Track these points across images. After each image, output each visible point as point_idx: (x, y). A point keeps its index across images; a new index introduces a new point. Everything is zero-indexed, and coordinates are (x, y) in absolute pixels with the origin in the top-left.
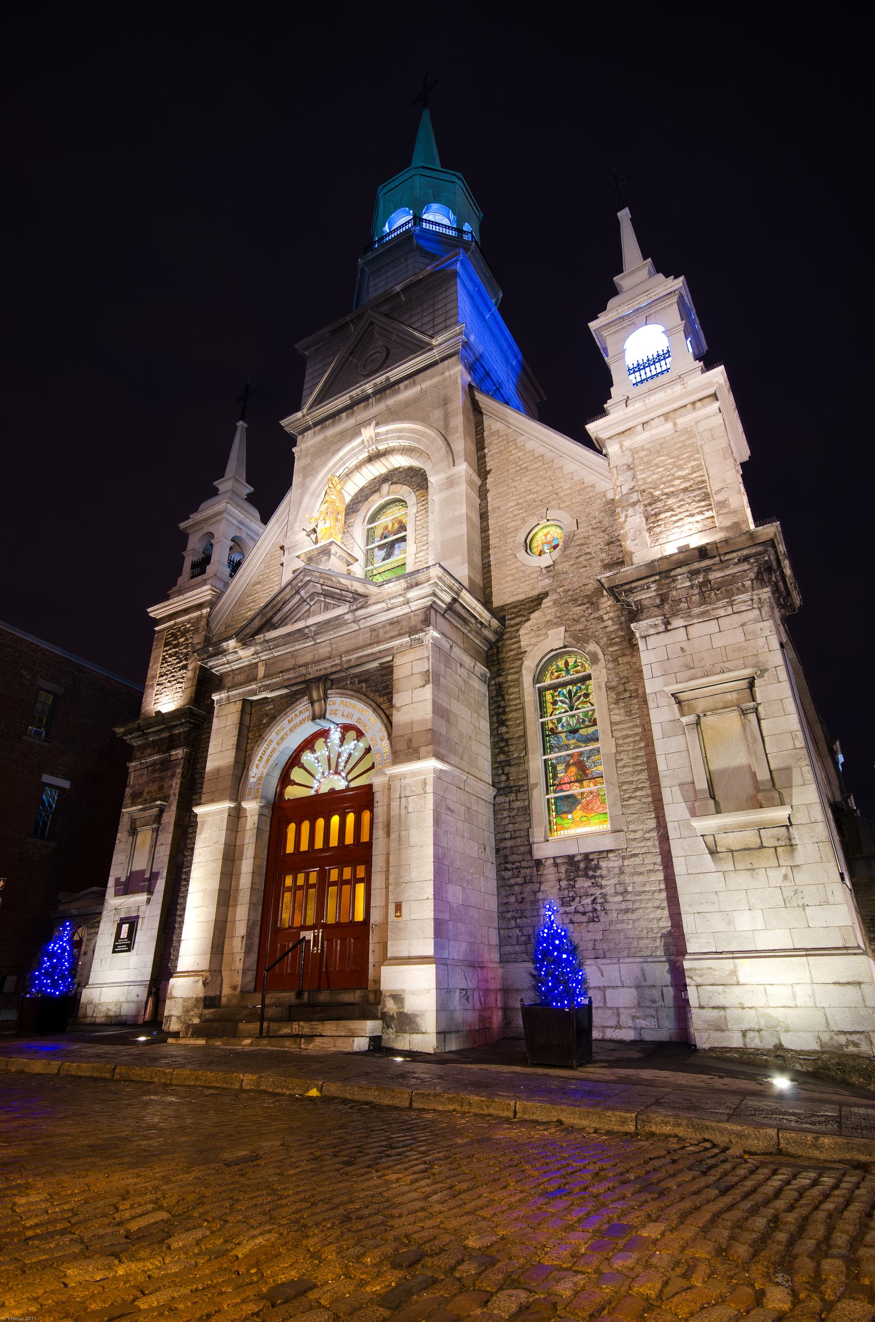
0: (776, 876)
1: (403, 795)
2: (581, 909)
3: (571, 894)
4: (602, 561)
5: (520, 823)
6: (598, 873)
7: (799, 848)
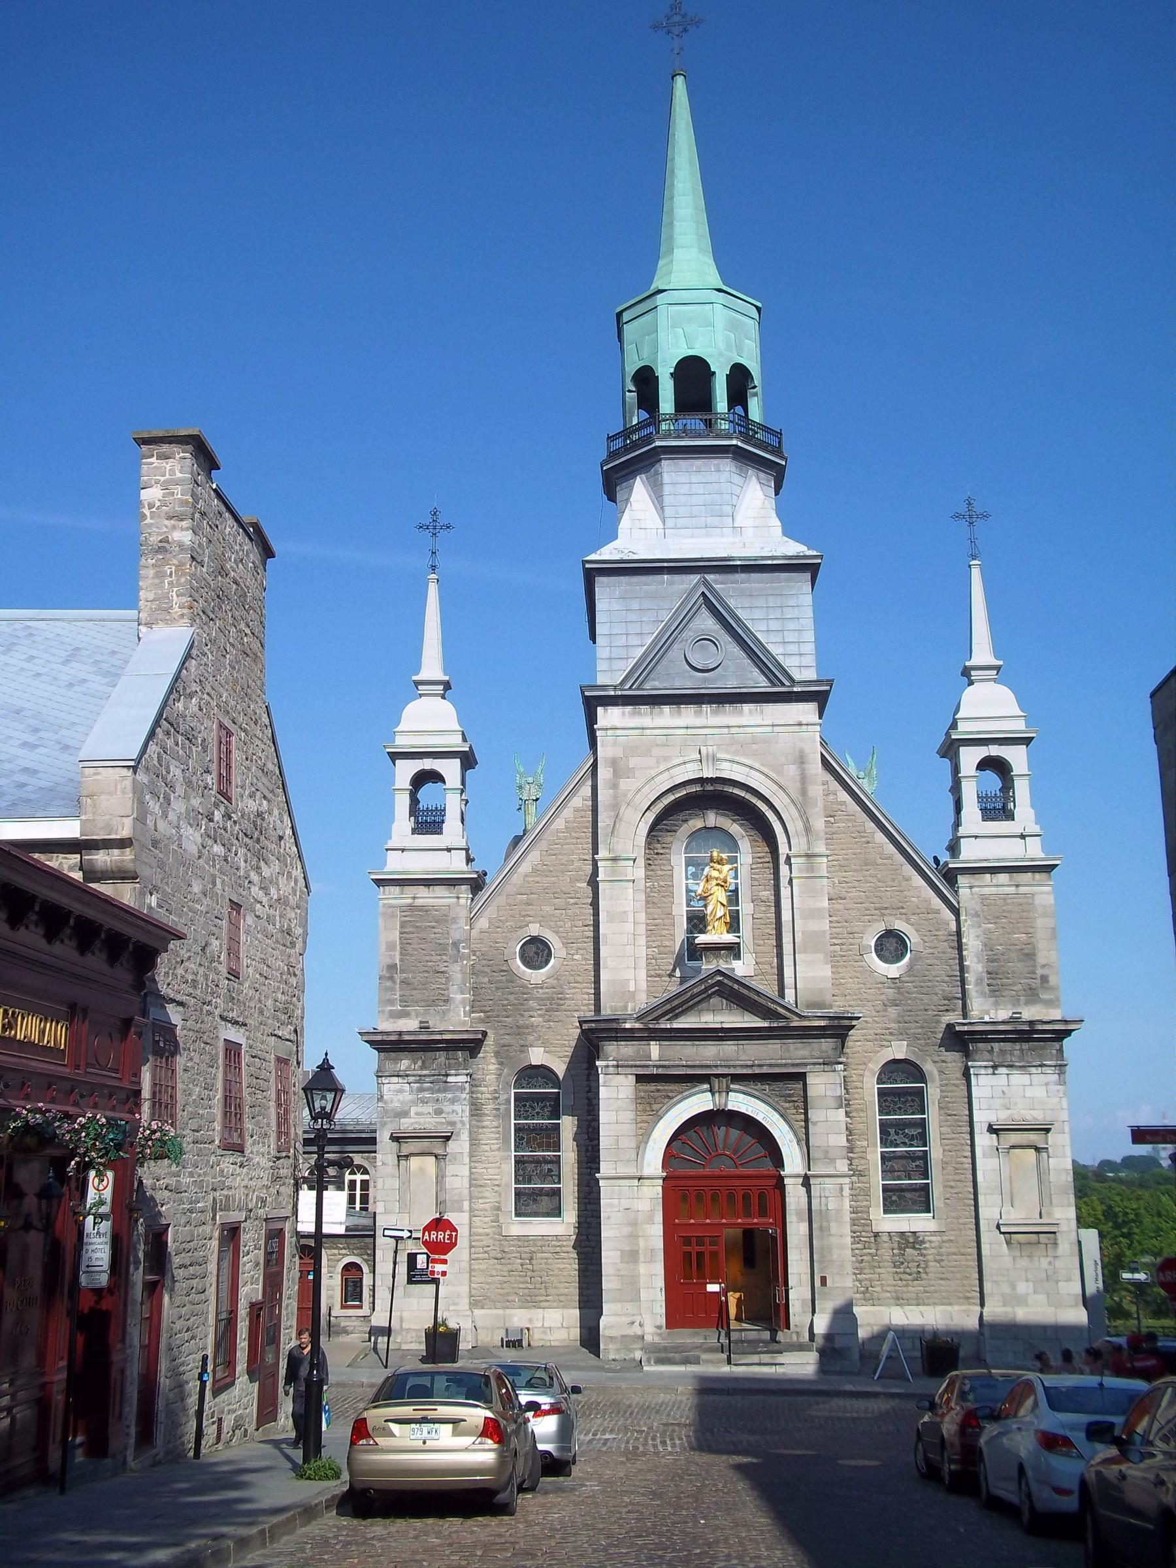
0: (1044, 1262)
1: (822, 1195)
2: (908, 1270)
3: (901, 1260)
4: (943, 990)
5: (862, 1201)
7: (1061, 1246)
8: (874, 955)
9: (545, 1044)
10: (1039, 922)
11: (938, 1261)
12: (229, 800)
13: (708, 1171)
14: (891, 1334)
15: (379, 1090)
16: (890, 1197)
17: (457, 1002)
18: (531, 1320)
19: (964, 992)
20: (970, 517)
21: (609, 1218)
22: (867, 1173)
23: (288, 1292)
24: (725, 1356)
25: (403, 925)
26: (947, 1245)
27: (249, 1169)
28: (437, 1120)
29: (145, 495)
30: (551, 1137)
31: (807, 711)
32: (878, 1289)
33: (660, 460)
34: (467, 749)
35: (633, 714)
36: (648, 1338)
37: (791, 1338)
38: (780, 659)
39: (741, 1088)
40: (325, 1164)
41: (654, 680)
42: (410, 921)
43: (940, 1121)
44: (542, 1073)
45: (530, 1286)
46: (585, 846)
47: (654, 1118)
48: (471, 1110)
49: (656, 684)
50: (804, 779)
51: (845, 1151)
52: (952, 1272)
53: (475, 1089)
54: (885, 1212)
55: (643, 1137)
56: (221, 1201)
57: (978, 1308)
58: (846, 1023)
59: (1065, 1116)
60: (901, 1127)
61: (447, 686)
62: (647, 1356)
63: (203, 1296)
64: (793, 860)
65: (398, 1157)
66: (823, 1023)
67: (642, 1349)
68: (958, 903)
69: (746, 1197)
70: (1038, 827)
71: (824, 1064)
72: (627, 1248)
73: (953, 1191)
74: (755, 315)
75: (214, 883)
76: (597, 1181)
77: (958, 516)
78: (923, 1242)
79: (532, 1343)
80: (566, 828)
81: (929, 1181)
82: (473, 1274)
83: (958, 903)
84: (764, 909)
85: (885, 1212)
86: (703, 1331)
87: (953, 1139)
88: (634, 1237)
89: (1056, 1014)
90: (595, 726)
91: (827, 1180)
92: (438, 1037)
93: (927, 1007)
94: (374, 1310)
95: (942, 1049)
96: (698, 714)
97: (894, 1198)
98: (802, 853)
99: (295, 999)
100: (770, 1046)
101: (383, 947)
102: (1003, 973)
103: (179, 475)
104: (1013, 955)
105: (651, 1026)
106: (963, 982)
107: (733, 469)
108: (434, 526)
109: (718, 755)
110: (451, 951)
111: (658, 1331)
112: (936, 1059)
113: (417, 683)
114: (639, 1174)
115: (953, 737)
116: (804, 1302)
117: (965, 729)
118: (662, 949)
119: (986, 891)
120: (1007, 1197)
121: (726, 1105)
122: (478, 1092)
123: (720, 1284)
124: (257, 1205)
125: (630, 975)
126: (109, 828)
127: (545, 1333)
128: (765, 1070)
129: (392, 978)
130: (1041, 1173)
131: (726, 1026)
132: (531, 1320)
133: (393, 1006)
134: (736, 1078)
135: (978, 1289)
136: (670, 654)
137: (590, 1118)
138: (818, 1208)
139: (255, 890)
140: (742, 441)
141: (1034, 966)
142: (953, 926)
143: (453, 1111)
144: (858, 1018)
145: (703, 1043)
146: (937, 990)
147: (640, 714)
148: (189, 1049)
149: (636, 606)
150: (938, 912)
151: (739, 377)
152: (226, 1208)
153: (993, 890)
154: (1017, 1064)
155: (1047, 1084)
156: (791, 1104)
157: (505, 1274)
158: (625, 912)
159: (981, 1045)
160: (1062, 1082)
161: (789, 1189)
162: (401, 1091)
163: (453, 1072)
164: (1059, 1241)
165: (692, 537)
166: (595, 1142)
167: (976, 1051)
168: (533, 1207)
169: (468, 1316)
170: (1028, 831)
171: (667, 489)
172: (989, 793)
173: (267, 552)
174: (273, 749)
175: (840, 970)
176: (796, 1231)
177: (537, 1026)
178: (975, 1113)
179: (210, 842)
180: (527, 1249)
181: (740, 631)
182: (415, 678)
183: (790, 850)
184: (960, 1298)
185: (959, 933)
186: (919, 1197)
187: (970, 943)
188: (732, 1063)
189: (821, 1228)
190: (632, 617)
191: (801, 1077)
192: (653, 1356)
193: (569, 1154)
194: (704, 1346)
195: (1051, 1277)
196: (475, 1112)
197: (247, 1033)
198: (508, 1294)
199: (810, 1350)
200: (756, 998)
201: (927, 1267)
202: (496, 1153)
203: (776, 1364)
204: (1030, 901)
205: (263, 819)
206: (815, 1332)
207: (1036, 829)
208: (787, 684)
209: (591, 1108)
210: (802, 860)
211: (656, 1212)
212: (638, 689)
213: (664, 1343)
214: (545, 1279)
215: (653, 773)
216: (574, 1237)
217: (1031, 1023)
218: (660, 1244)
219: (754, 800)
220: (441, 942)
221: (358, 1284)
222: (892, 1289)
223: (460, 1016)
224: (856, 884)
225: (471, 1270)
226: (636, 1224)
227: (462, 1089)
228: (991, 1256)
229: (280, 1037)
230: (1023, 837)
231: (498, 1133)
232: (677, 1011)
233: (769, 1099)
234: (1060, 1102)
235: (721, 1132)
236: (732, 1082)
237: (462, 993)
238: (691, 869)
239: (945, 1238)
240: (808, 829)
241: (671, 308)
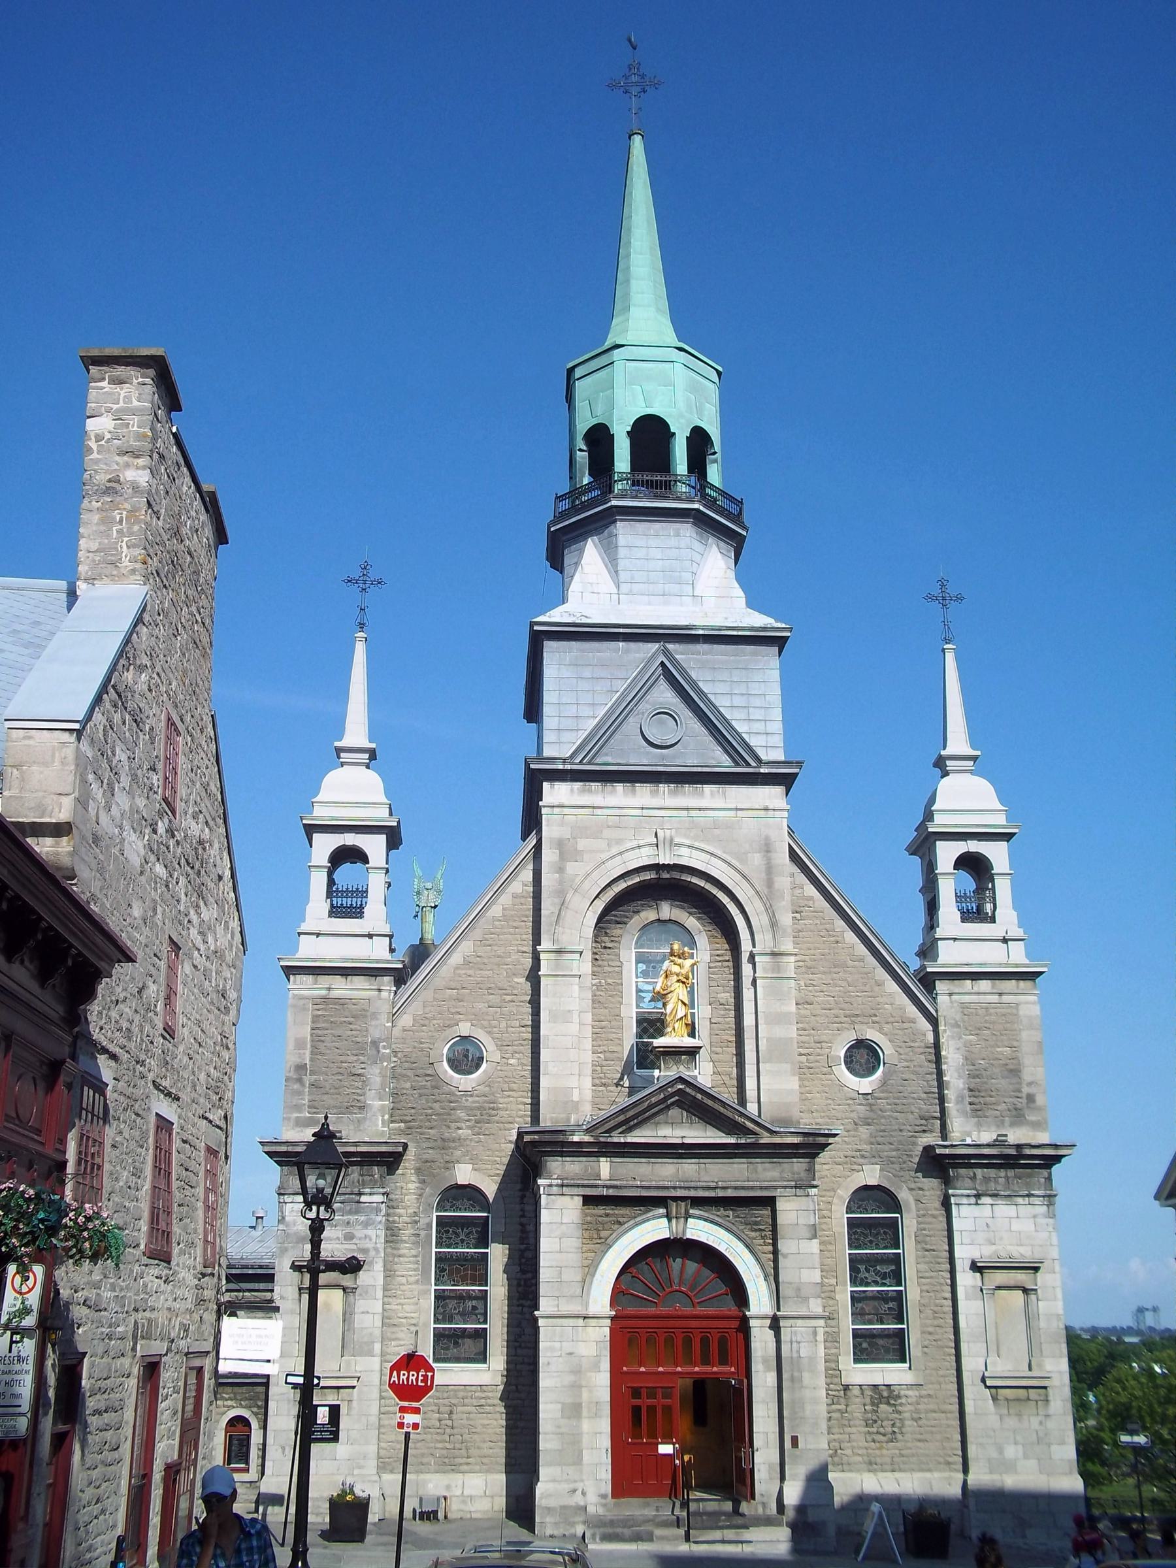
0: (1035, 1421)
1: (794, 1339)
2: (881, 1430)
3: (874, 1417)
4: (920, 1109)
6: (900, 1401)
7: (1052, 1403)
8: (843, 1066)
9: (474, 1160)
10: (1025, 1035)
11: (915, 1420)
12: (173, 812)
13: (664, 1310)
14: (875, 1507)
15: (281, 1210)
16: (860, 1344)
17: (375, 1110)
18: (448, 1487)
19: (943, 1111)
20: (944, 599)
21: (549, 1364)
22: (835, 1316)
23: (204, 1451)
24: (682, 1532)
25: (315, 1019)
26: (926, 1400)
27: (174, 1286)
28: (347, 1246)
29: (91, 425)
30: (477, 1269)
31: (773, 795)
32: (848, 1452)
33: (615, 521)
34: (395, 824)
35: (583, 791)
36: (591, 1509)
37: (756, 1510)
38: (744, 736)
39: (702, 1213)
40: (322, 1267)
41: (606, 755)
42: (324, 1016)
43: (917, 1257)
44: (470, 1193)
45: (447, 1445)
46: (524, 937)
47: (603, 1247)
48: (386, 1236)
49: (609, 759)
50: (769, 869)
51: (818, 1288)
52: (932, 1433)
53: (391, 1211)
54: (856, 1361)
55: (590, 1269)
56: (143, 1326)
57: (961, 1476)
58: (822, 1140)
59: (1055, 1253)
60: (873, 1264)
61: (373, 755)
62: (592, 1531)
63: (116, 1455)
64: (757, 959)
65: (300, 1289)
66: (796, 1140)
67: (584, 1523)
68: (937, 1011)
69: (705, 1342)
70: (1021, 930)
71: (796, 1187)
72: (569, 1400)
73: (930, 1337)
74: (715, 378)
75: (155, 911)
76: (536, 1320)
77: (931, 597)
78: (899, 1397)
79: (449, 1515)
80: (504, 916)
81: (904, 1326)
82: (382, 1430)
83: (937, 1011)
84: (722, 1012)
85: (856, 1361)
86: (654, 1502)
87: (931, 1277)
88: (576, 1387)
89: (1043, 1138)
90: (541, 803)
91: (800, 1322)
92: (352, 1149)
93: (902, 1127)
94: (263, 1474)
95: (919, 1175)
96: (655, 793)
97: (865, 1345)
98: (768, 950)
99: (226, 1078)
100: (735, 1166)
101: (291, 1045)
102: (986, 1090)
103: (136, 403)
104: (997, 1070)
105: (602, 1139)
106: (942, 1099)
107: (694, 535)
108: (363, 581)
109: (677, 840)
110: (370, 1051)
111: (603, 1501)
112: (913, 1186)
113: (339, 751)
114: (584, 1312)
115: (930, 830)
116: (770, 1466)
117: (941, 822)
118: (608, 1054)
119: (967, 998)
120: (992, 1346)
121: (684, 1232)
122: (395, 1215)
123: (674, 1444)
124: (180, 1334)
125: (573, 1082)
126: (41, 809)
127: (464, 1502)
128: (730, 1193)
129: (300, 1081)
130: (1029, 1318)
131: (686, 1141)
132: (448, 1487)
133: (300, 1113)
134: (697, 1202)
135: (960, 1453)
136: (624, 727)
137: (523, 1247)
138: (789, 1355)
139: (194, 932)
140: (705, 506)
141: (1020, 1083)
142: (930, 1038)
143: (366, 1237)
144: (835, 1135)
145: (660, 1160)
146: (913, 1108)
147: (590, 791)
148: (119, 1119)
149: (587, 673)
150: (913, 1021)
151: (699, 440)
152: (147, 1337)
153: (974, 998)
154: (1002, 1193)
155: (1035, 1217)
156: (758, 1234)
158: (569, 1011)
159: (962, 1171)
160: (1053, 1216)
161: (755, 1332)
163: (367, 1190)
164: (1051, 1398)
165: (649, 604)
166: (529, 1275)
167: (957, 1177)
168: (454, 1351)
169: (376, 1482)
170: (1010, 935)
171: (622, 552)
172: (967, 892)
173: (221, 536)
174: (216, 769)
175: (806, 1083)
176: (763, 1381)
177: (465, 1140)
178: (957, 1248)
179: (153, 858)
180: (446, 1402)
181: (702, 705)
182: (337, 744)
183: (754, 946)
184: (940, 1463)
185: (937, 1045)
186: (892, 1344)
187: (949, 1056)
188: (693, 1184)
189: (792, 1379)
190: (583, 685)
191: (770, 1202)
192: (599, 1531)
193: (498, 1289)
194: (658, 1520)
195: (1042, 1440)
196: (391, 1238)
197: (179, 1110)
198: (423, 1455)
199: (780, 1524)
200: (722, 1110)
201: (903, 1426)
202: (414, 1286)
203: (742, 1542)
204: (1014, 1011)
205: (204, 849)
206: (786, 1502)
207: (1018, 932)
208: (753, 764)
209: (524, 1236)
210: (767, 958)
211: (603, 1358)
212: (589, 763)
213: (610, 1516)
214: (466, 1437)
215: (604, 856)
216: (501, 1387)
217: (1019, 1147)
218: (605, 1395)
219: (715, 891)
220: (359, 1040)
221: (245, 1442)
222: (865, 1451)
224: (824, 988)
225: (380, 1426)
226: (580, 1372)
227: (378, 1211)
228: (975, 1414)
229: (210, 1122)
230: (1005, 941)
231: (417, 1262)
232: (632, 1123)
233: (734, 1228)
234: (1050, 1237)
235: (676, 1264)
236: (692, 1206)
237: (381, 1099)
238: (642, 967)
239: (924, 1393)
240: (774, 924)
241: (629, 364)
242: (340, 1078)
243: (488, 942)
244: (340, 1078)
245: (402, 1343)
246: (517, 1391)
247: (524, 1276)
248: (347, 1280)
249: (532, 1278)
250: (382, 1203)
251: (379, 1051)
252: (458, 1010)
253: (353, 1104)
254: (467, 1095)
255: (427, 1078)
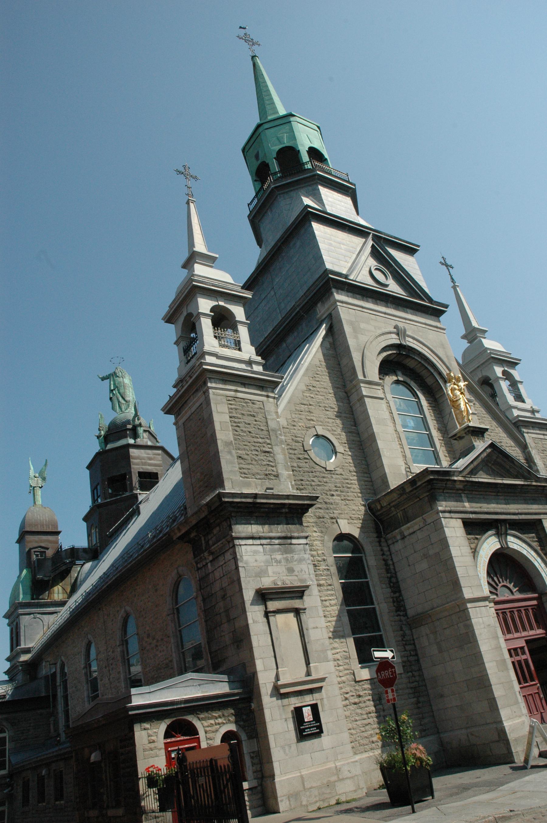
42: (236, 409)
105: (467, 479)
137: (389, 575)
157: (365, 716)
158: (385, 419)
162: (256, 552)
166: (397, 594)
209: (388, 567)
223: (289, 488)
242: (256, 453)
243: (317, 379)
244: (256, 453)
245: (338, 651)
246: (413, 676)
247: (395, 595)
248: (296, 603)
249: (400, 596)
250: (307, 544)
251: (277, 437)
252: (312, 418)
253: (270, 472)
254: (331, 474)
255: (305, 461)
